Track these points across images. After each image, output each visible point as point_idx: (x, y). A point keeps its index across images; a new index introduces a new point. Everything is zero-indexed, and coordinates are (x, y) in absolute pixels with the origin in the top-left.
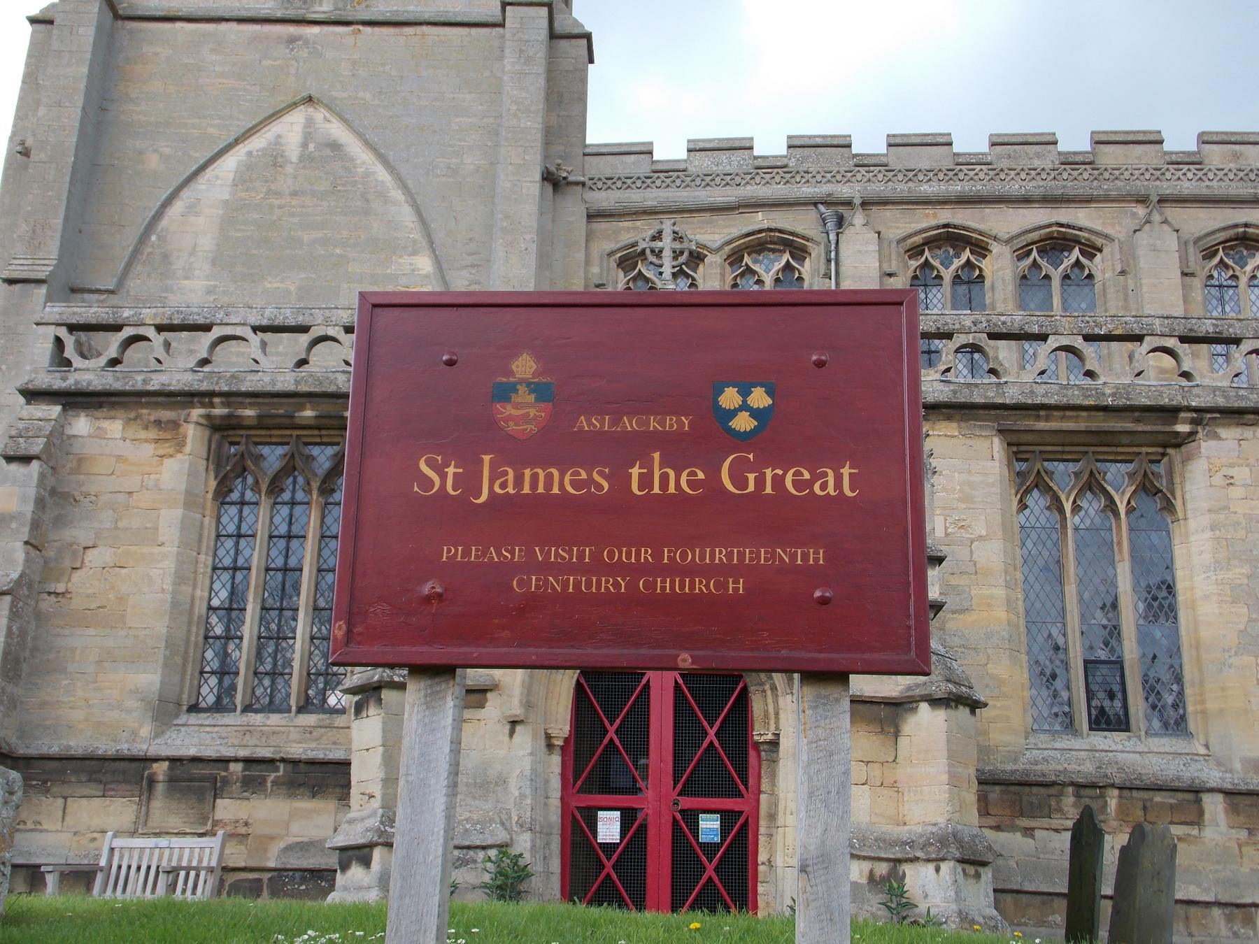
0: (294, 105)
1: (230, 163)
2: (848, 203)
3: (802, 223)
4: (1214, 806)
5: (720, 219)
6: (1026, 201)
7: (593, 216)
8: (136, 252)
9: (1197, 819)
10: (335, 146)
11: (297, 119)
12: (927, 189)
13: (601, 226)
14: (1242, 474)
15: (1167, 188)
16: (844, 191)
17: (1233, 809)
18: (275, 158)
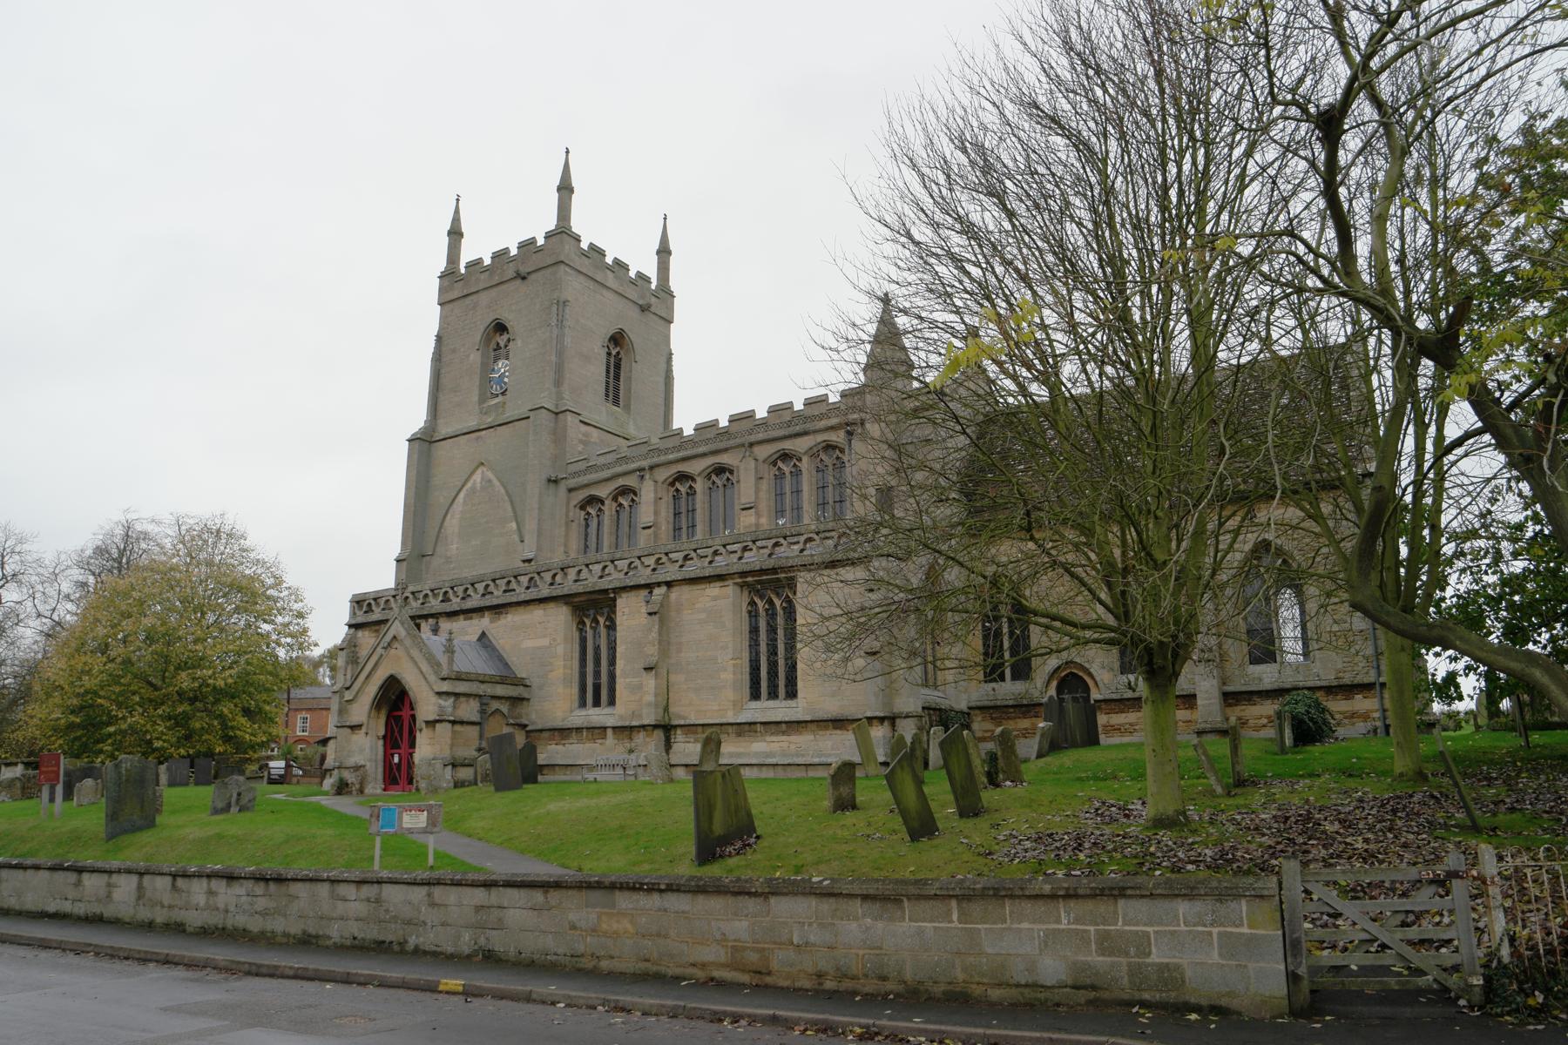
0: (477, 467)
1: (462, 495)
2: (644, 469)
3: (631, 481)
4: (609, 732)
5: (609, 483)
6: (704, 455)
7: (570, 490)
8: (438, 537)
9: (604, 738)
10: (490, 481)
11: (479, 471)
12: (671, 457)
13: (573, 494)
14: (626, 610)
15: (753, 438)
16: (645, 463)
17: (614, 733)
18: (473, 489)
